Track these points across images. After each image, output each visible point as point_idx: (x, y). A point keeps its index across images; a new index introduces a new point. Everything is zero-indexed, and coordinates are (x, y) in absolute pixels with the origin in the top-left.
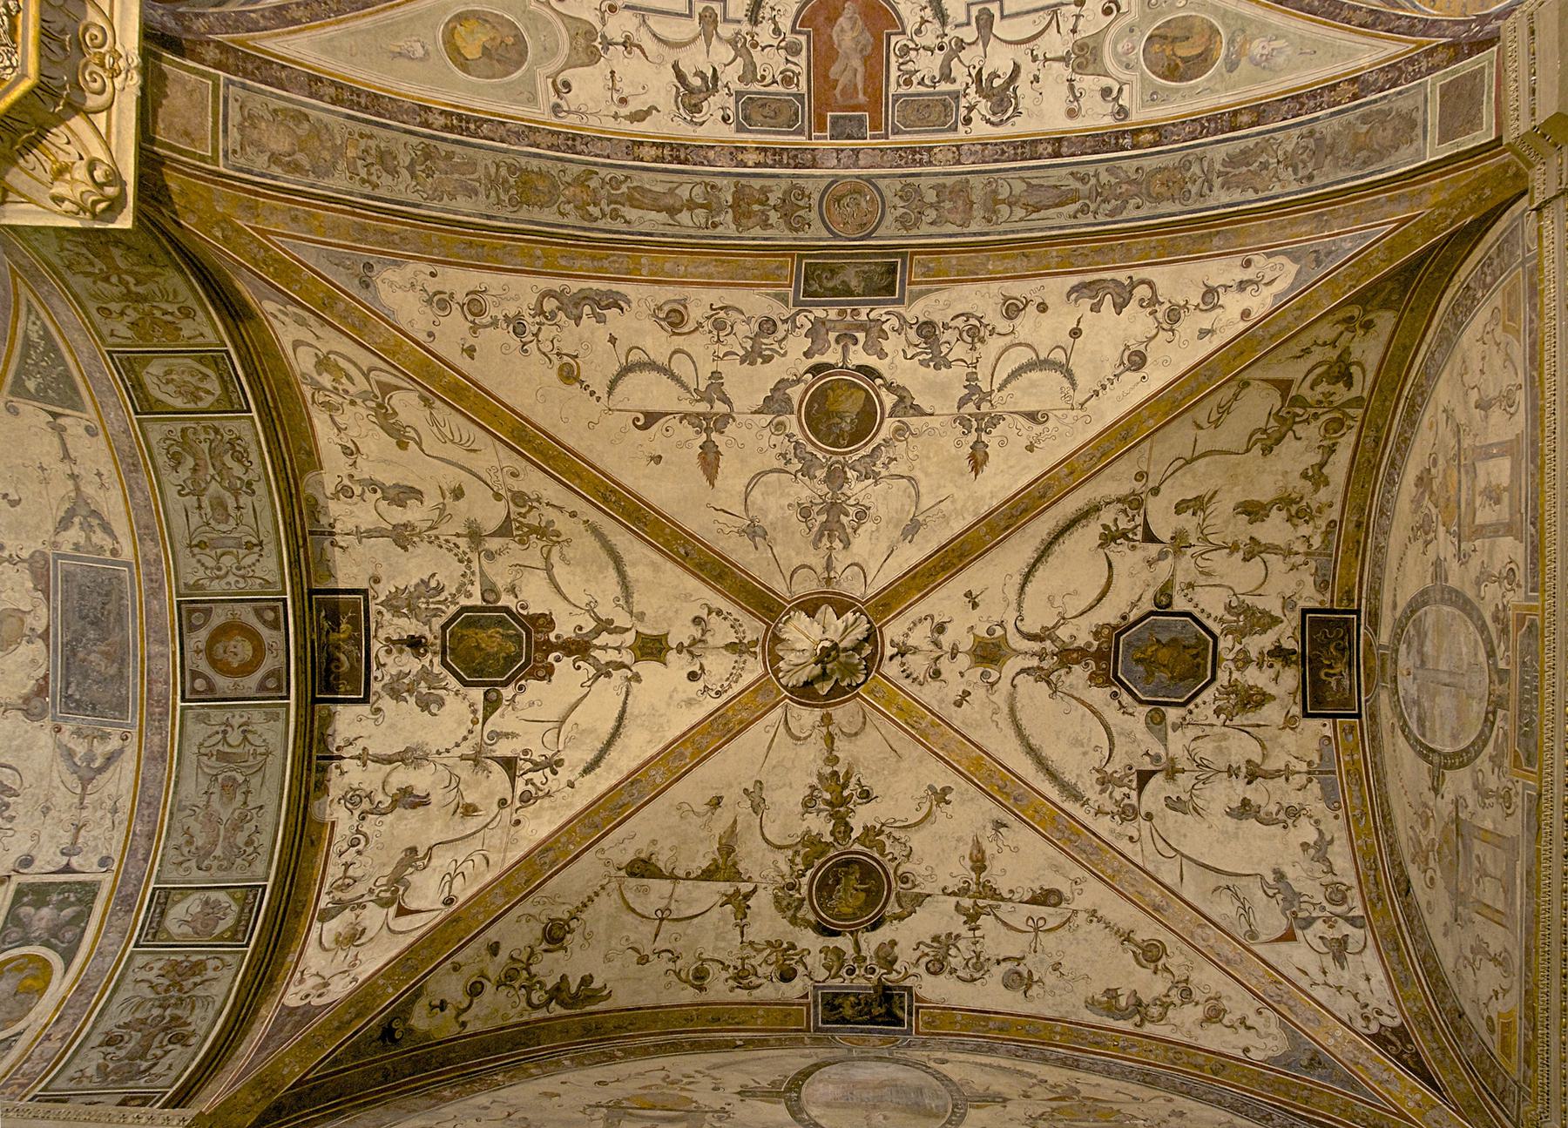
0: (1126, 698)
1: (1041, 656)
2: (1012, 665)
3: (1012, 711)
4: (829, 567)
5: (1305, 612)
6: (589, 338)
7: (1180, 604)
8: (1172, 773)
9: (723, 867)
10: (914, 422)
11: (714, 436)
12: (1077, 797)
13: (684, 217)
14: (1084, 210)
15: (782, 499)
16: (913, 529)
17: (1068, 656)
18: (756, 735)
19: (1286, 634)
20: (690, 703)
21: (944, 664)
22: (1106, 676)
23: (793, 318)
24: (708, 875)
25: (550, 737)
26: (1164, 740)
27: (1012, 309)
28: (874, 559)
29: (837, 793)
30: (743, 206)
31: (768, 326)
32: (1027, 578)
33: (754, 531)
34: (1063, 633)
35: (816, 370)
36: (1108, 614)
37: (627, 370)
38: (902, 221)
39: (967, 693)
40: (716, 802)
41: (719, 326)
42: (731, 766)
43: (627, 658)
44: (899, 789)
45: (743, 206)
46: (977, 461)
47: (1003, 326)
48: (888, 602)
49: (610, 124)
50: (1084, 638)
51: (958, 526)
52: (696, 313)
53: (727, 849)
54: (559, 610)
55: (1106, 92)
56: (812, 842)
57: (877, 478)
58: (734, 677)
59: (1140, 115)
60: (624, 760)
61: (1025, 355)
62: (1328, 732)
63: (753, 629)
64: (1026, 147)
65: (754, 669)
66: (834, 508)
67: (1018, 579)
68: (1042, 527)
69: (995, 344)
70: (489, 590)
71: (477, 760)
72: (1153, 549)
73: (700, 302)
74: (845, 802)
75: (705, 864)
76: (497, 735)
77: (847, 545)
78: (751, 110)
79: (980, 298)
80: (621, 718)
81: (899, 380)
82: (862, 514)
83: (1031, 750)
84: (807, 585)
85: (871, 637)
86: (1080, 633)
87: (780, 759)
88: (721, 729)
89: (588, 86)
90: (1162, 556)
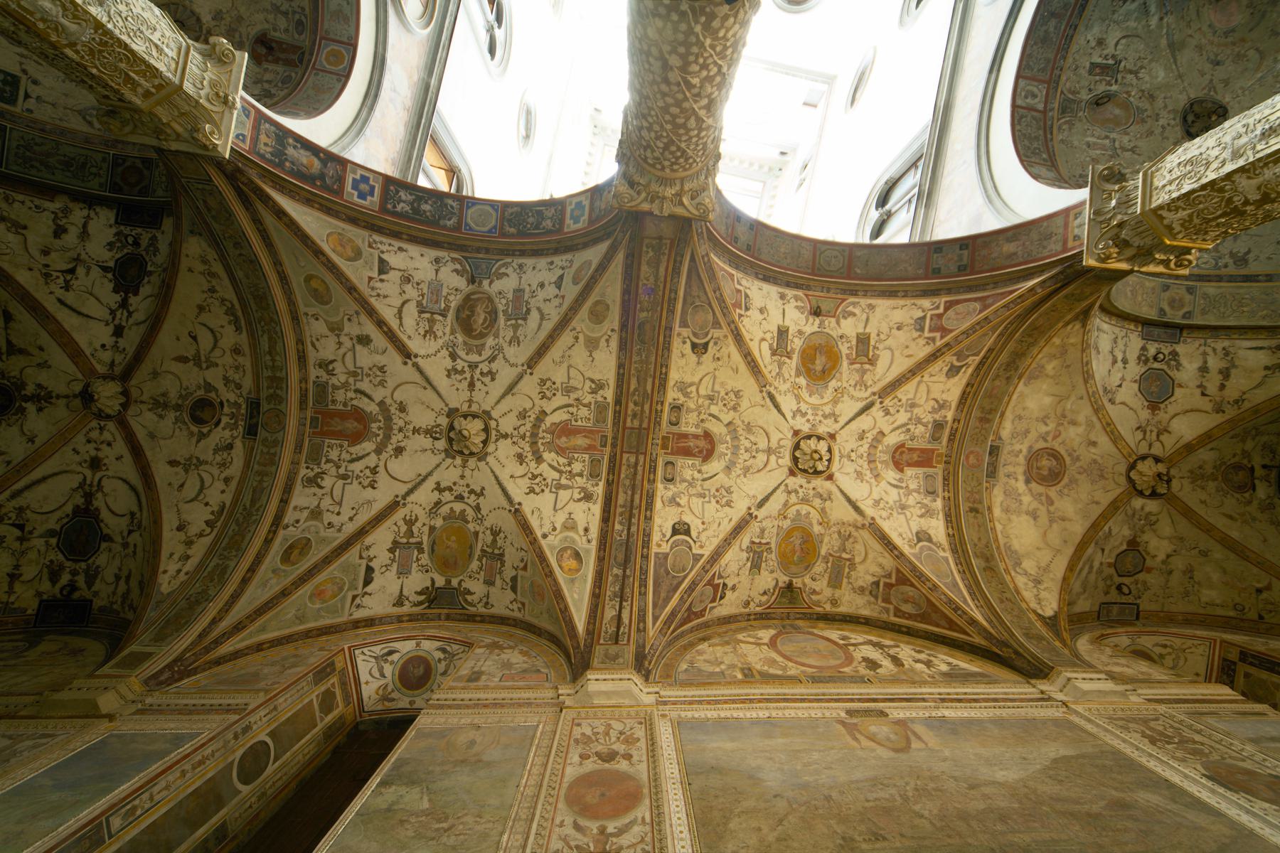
0: (65, 521)
1: (91, 485)
2: (88, 473)
3: (66, 472)
4: (142, 402)
5: (91, 601)
6: (217, 318)
7: (104, 545)
8: (21, 540)
9: (12, 349)
10: (194, 440)
11: (191, 363)
12: (14, 495)
13: (268, 357)
14: (245, 509)
15: (169, 385)
16: (152, 436)
17: (89, 497)
18: (71, 368)
19: (83, 592)
20: (90, 344)
21: (93, 445)
22: (77, 510)
23: (241, 396)
24: (9, 342)
25: (83, 288)
26: (41, 536)
27: (227, 480)
28: (142, 421)
29: (43, 398)
30: (273, 379)
31: (239, 386)
32: (125, 481)
33: (155, 374)
34: (99, 495)
35: (222, 404)
36: (104, 514)
37: (212, 331)
38: (266, 440)
39: (78, 453)
40: (41, 349)
41: (237, 368)
42: (59, 358)
43: (117, 322)
44: (38, 422)
45: (273, 379)
46: (173, 463)
47: (223, 476)
48: (123, 424)
49: (308, 334)
50: (96, 503)
51: (148, 454)
52: (240, 359)
53: (22, 352)
54: (139, 298)
55: (298, 521)
56: (23, 385)
57: (175, 423)
58: (99, 361)
59: (281, 533)
60: (64, 316)
61: (207, 484)
62: (29, 612)
63: (118, 370)
64: (288, 489)
65: (101, 369)
66: (165, 406)
67: (124, 477)
68: (140, 488)
69: (216, 472)
70: (151, 273)
71: (77, 259)
72: (125, 534)
73: (246, 362)
74: (39, 401)
75: (14, 341)
76: (89, 269)
77: (150, 410)
78: (322, 388)
79: (235, 469)
80: (87, 316)
81: (212, 435)
82: (161, 417)
83: (44, 479)
84: (134, 393)
85: (108, 417)
86: (98, 502)
87: (60, 374)
88: (75, 354)
89: (319, 327)
90: (123, 538)
